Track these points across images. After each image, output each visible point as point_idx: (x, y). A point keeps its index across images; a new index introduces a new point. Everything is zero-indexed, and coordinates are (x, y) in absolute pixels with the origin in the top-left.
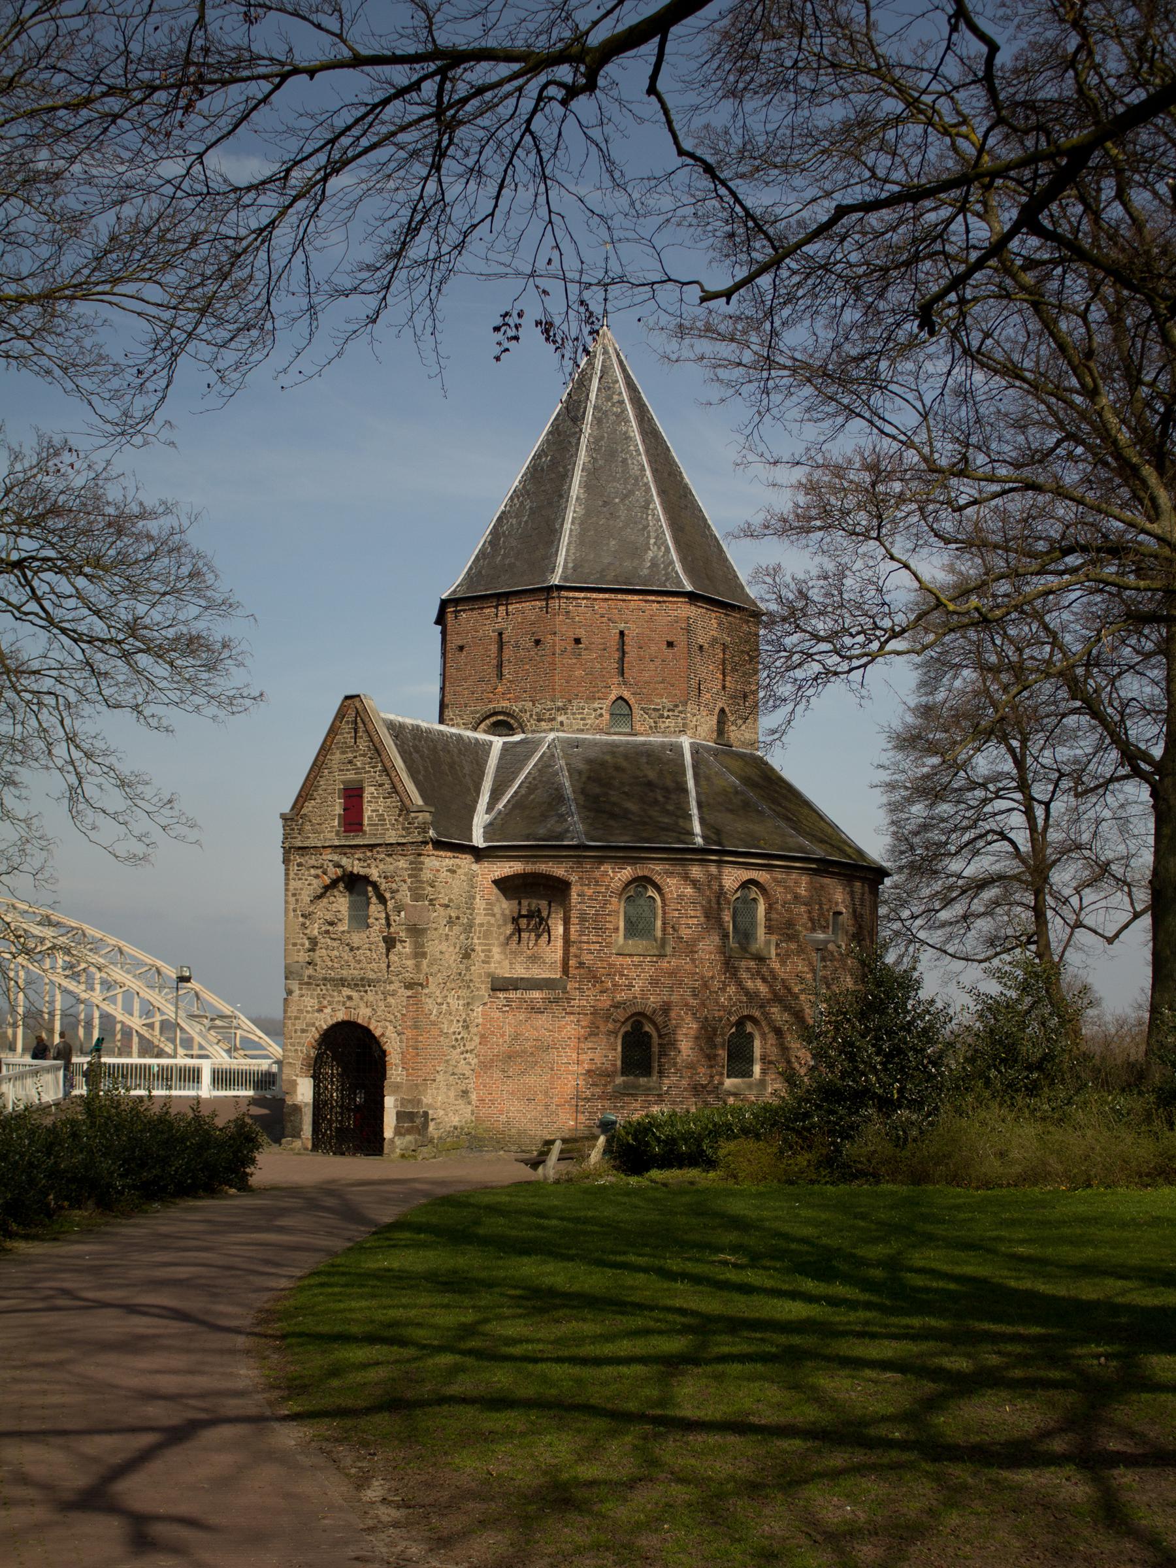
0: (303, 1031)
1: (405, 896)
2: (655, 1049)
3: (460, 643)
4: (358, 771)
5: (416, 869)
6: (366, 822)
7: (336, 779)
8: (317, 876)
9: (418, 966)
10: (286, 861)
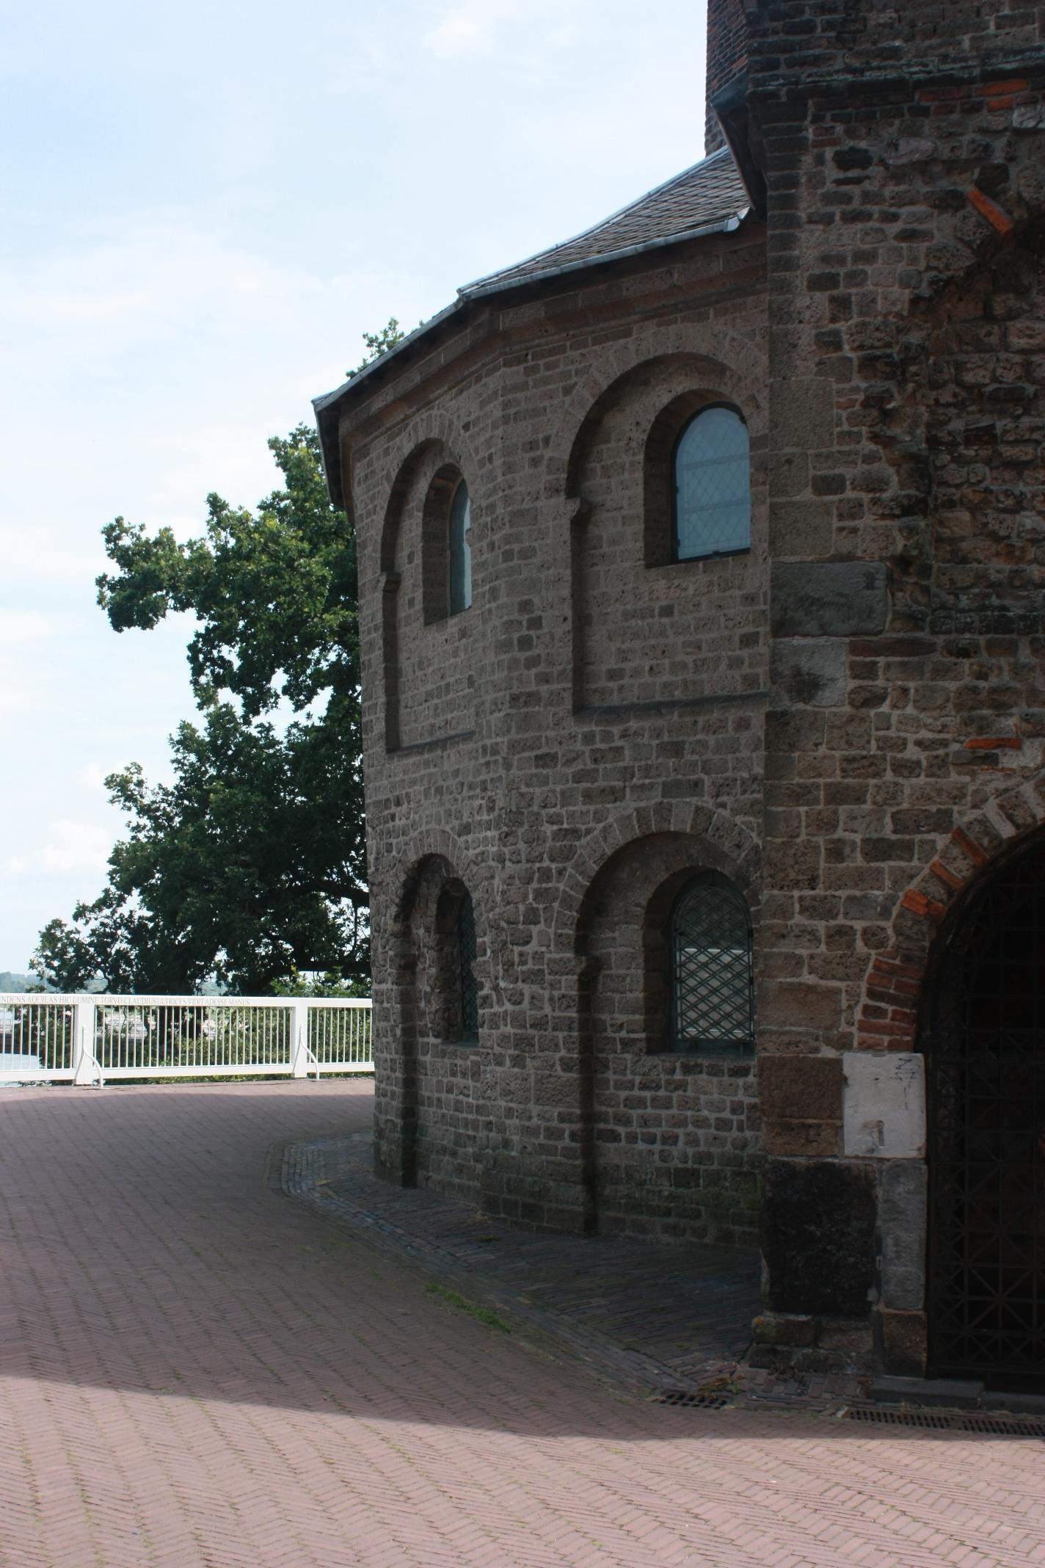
0: (877, 849)
8: (951, 201)
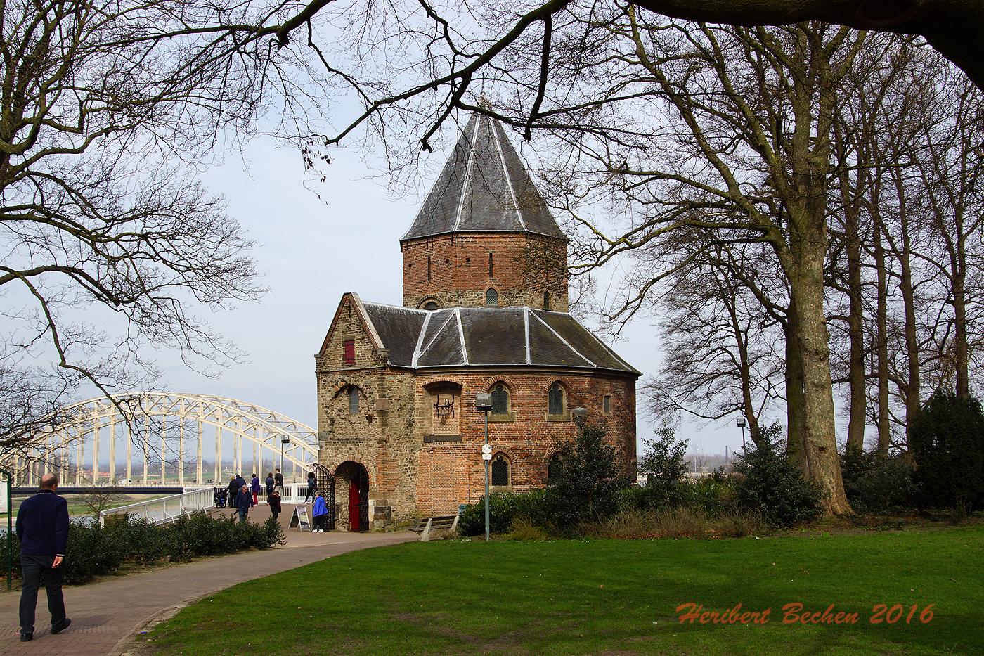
1: (376, 396)
2: (510, 471)
3: (410, 263)
4: (351, 332)
5: (382, 380)
6: (356, 358)
7: (341, 336)
8: (333, 387)
9: (383, 431)
10: (318, 379)
